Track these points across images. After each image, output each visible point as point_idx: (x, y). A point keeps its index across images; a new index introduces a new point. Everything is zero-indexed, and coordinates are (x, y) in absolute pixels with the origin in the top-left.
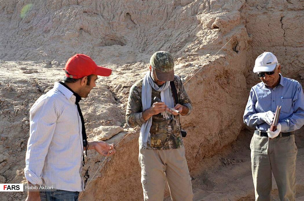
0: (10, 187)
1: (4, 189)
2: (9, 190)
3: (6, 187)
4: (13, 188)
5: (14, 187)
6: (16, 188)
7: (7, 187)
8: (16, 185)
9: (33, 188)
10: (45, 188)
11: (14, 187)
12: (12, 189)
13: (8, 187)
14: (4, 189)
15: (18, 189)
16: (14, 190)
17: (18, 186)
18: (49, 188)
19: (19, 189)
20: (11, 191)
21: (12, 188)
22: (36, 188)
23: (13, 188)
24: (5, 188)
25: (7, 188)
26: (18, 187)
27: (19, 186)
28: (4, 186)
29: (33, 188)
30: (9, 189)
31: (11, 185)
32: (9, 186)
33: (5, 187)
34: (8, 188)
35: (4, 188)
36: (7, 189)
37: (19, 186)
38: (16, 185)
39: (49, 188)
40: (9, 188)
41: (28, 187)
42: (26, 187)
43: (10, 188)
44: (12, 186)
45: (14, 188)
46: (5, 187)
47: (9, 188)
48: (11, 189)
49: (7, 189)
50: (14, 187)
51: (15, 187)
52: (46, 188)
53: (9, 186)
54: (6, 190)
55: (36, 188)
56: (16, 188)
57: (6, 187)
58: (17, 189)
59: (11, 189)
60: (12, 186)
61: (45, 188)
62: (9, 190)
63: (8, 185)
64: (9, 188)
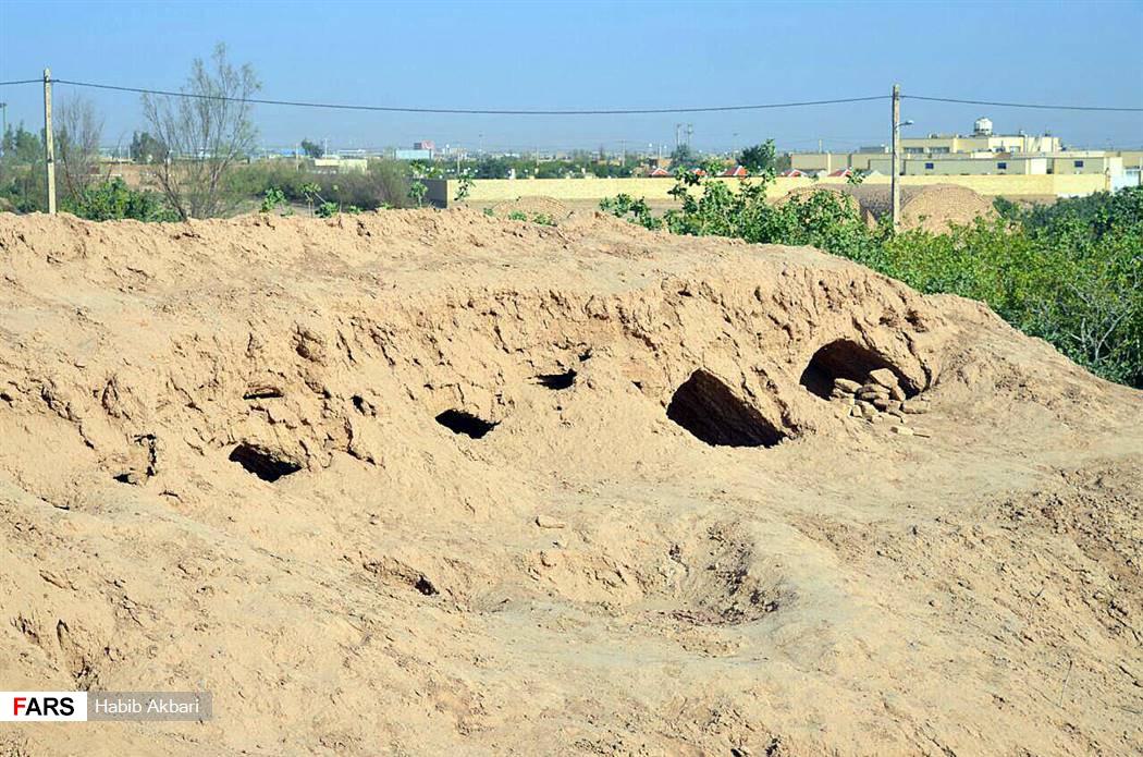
0: (37, 705)
1: (16, 713)
3: (23, 706)
4: (49, 709)
5: (52, 703)
6: (59, 707)
7: (27, 703)
9: (123, 708)
10: (168, 708)
11: (52, 703)
12: (46, 713)
13: (31, 704)
14: (16, 713)
15: (67, 710)
17: (67, 702)
19: (72, 710)
21: (46, 707)
22: (137, 708)
23: (49, 709)
24: (19, 710)
25: (26, 709)
26: (68, 706)
27: (71, 701)
28: (16, 700)
29: (123, 708)
30: (34, 710)
32: (34, 700)
33: (19, 703)
34: (30, 709)
35: (16, 706)
36: (28, 713)
37: (71, 701)
39: (184, 710)
40: (34, 707)
42: (97, 705)
43: (37, 709)
44: (46, 700)
45: (52, 707)
46: (19, 703)
47: (34, 707)
48: (40, 714)
49: (28, 713)
50: (51, 703)
51: (56, 704)
52: (174, 709)
53: (34, 700)
55: (137, 708)
56: (59, 707)
57: (23, 706)
58: (62, 712)
59: (40, 714)
60: (46, 700)
61: (168, 708)
64: (33, 706)
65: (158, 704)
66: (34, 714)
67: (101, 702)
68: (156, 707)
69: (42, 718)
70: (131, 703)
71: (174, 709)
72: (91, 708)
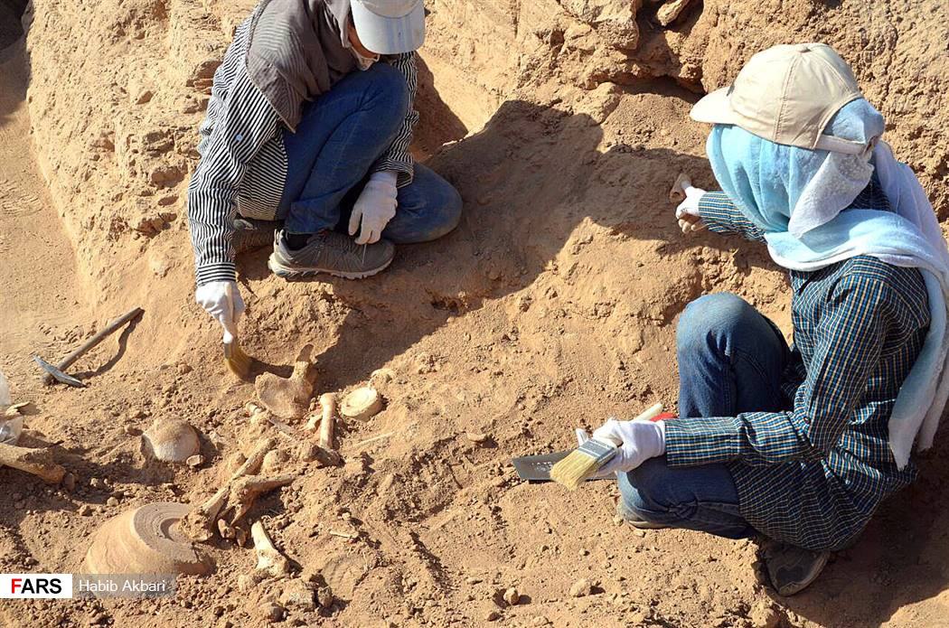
0: (30, 585)
1: (13, 592)
3: (19, 586)
4: (41, 588)
5: (43, 583)
6: (49, 587)
7: (22, 584)
9: (102, 588)
11: (43, 583)
12: (38, 592)
13: (26, 584)
14: (13, 592)
15: (56, 589)
17: (55, 583)
19: (60, 589)
20: (35, 596)
21: (38, 586)
22: (114, 587)
23: (41, 588)
24: (16, 589)
25: (21, 588)
27: (59, 582)
28: (13, 581)
29: (102, 588)
30: (28, 589)
31: (33, 577)
32: (28, 581)
33: (16, 583)
34: (25, 589)
35: (14, 586)
36: (23, 592)
37: (59, 582)
38: (49, 577)
40: (28, 586)
41: (88, 585)
43: (31, 589)
44: (38, 581)
45: (43, 587)
46: (16, 583)
47: (28, 586)
48: (33, 592)
49: (23, 592)
50: (42, 583)
51: (47, 584)
53: (28, 581)
54: (18, 594)
56: (49, 587)
57: (19, 586)
58: (52, 590)
59: (33, 592)
60: (38, 581)
62: (28, 594)
63: (24, 577)
64: (27, 586)
66: (28, 593)
68: (129, 586)
69: (35, 596)
72: (75, 585)
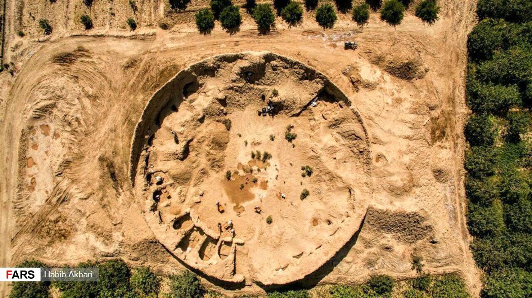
0: (17, 274)
1: (7, 278)
2: (16, 279)
3: (11, 274)
6: (27, 275)
7: (13, 273)
8: (28, 269)
10: (78, 275)
12: (21, 278)
13: (14, 274)
14: (7, 278)
15: (31, 276)
16: (24, 279)
17: (31, 273)
18: (85, 276)
19: (34, 276)
20: (20, 280)
21: (21, 275)
22: (64, 275)
25: (12, 276)
27: (33, 272)
28: (7, 271)
31: (19, 270)
32: (16, 272)
33: (9, 273)
34: (14, 276)
35: (8, 275)
36: (13, 278)
37: (33, 272)
39: (85, 276)
40: (16, 275)
41: (49, 274)
43: (17, 276)
44: (21, 271)
45: (24, 275)
46: (9, 273)
47: (16, 275)
48: (18, 278)
49: (13, 278)
50: (24, 273)
51: (26, 274)
52: (81, 275)
53: (16, 272)
54: (10, 279)
55: (64, 275)
56: (27, 275)
57: (11, 274)
58: (29, 277)
59: (18, 278)
60: (21, 271)
61: (78, 275)
62: (16, 279)
63: (14, 269)
64: (15, 274)
65: (74, 273)
67: (47, 272)
70: (61, 273)
71: (81, 275)
72: (42, 274)
